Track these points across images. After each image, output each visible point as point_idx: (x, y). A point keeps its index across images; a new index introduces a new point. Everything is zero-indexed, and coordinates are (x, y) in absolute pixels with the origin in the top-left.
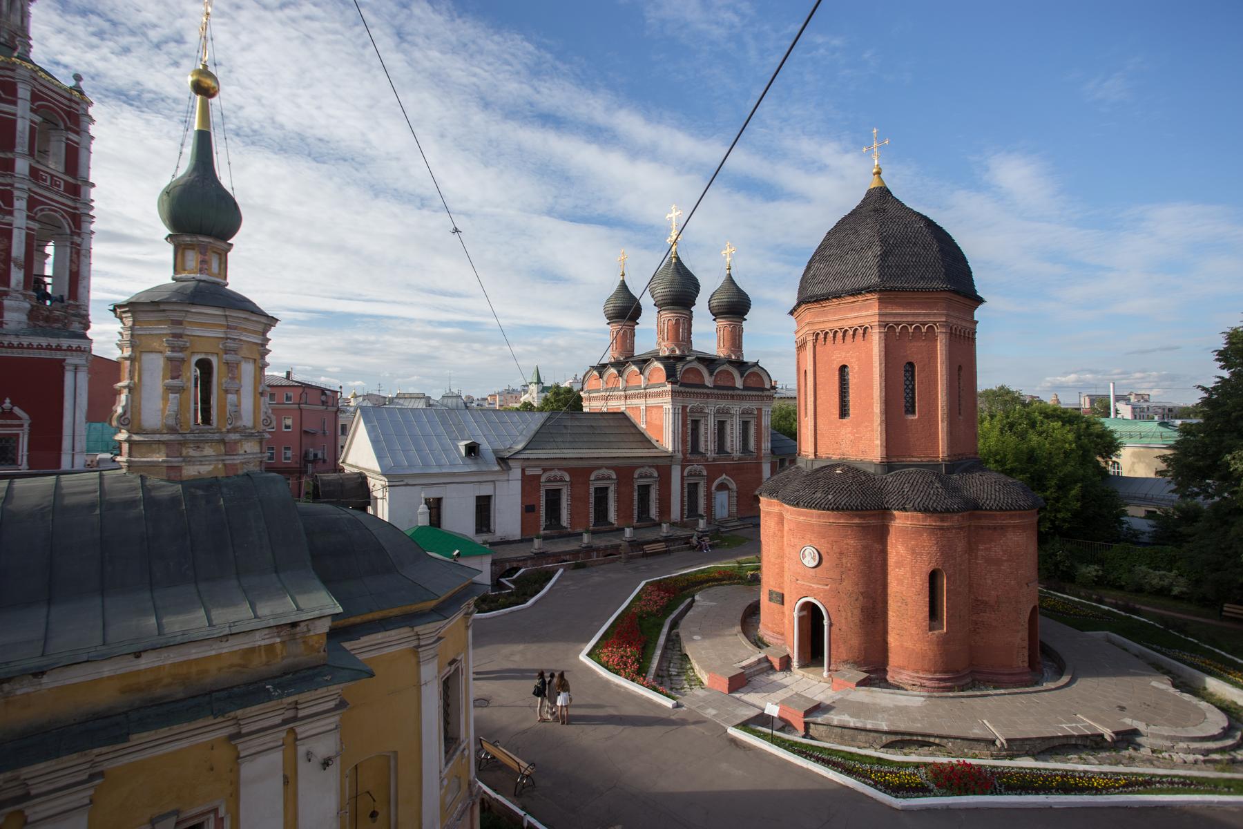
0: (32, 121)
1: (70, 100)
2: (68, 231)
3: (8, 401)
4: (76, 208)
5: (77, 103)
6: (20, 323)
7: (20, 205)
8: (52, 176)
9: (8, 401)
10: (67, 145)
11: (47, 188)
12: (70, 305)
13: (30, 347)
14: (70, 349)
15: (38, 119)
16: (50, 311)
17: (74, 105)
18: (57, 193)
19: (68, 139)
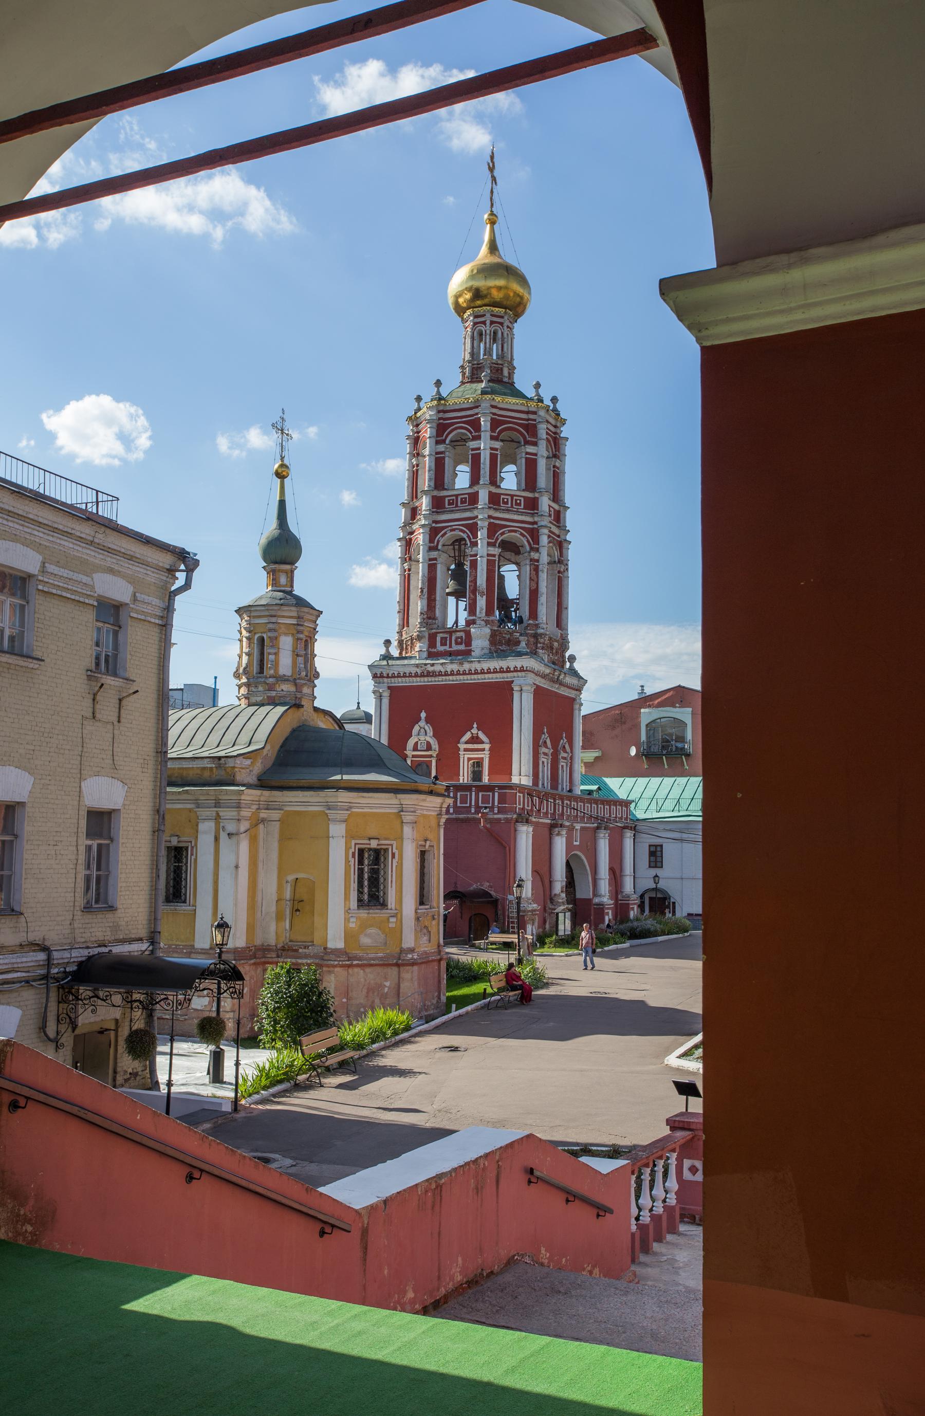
0: (492, 449)
1: (528, 413)
2: (528, 548)
3: (475, 726)
4: (535, 523)
5: (535, 413)
6: (483, 649)
7: (482, 534)
8: (512, 496)
9: (475, 726)
10: (526, 458)
11: (508, 511)
12: (529, 625)
13: (489, 672)
14: (516, 670)
15: (497, 445)
16: (511, 634)
17: (531, 416)
18: (517, 513)
19: (527, 453)
